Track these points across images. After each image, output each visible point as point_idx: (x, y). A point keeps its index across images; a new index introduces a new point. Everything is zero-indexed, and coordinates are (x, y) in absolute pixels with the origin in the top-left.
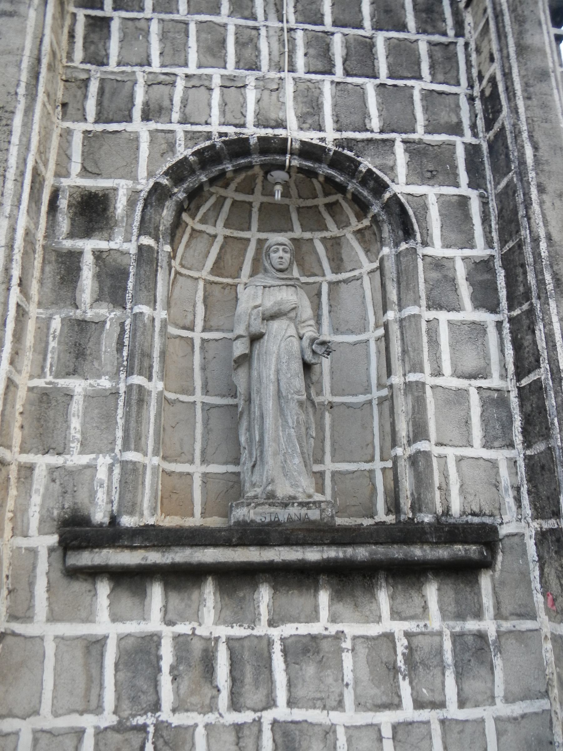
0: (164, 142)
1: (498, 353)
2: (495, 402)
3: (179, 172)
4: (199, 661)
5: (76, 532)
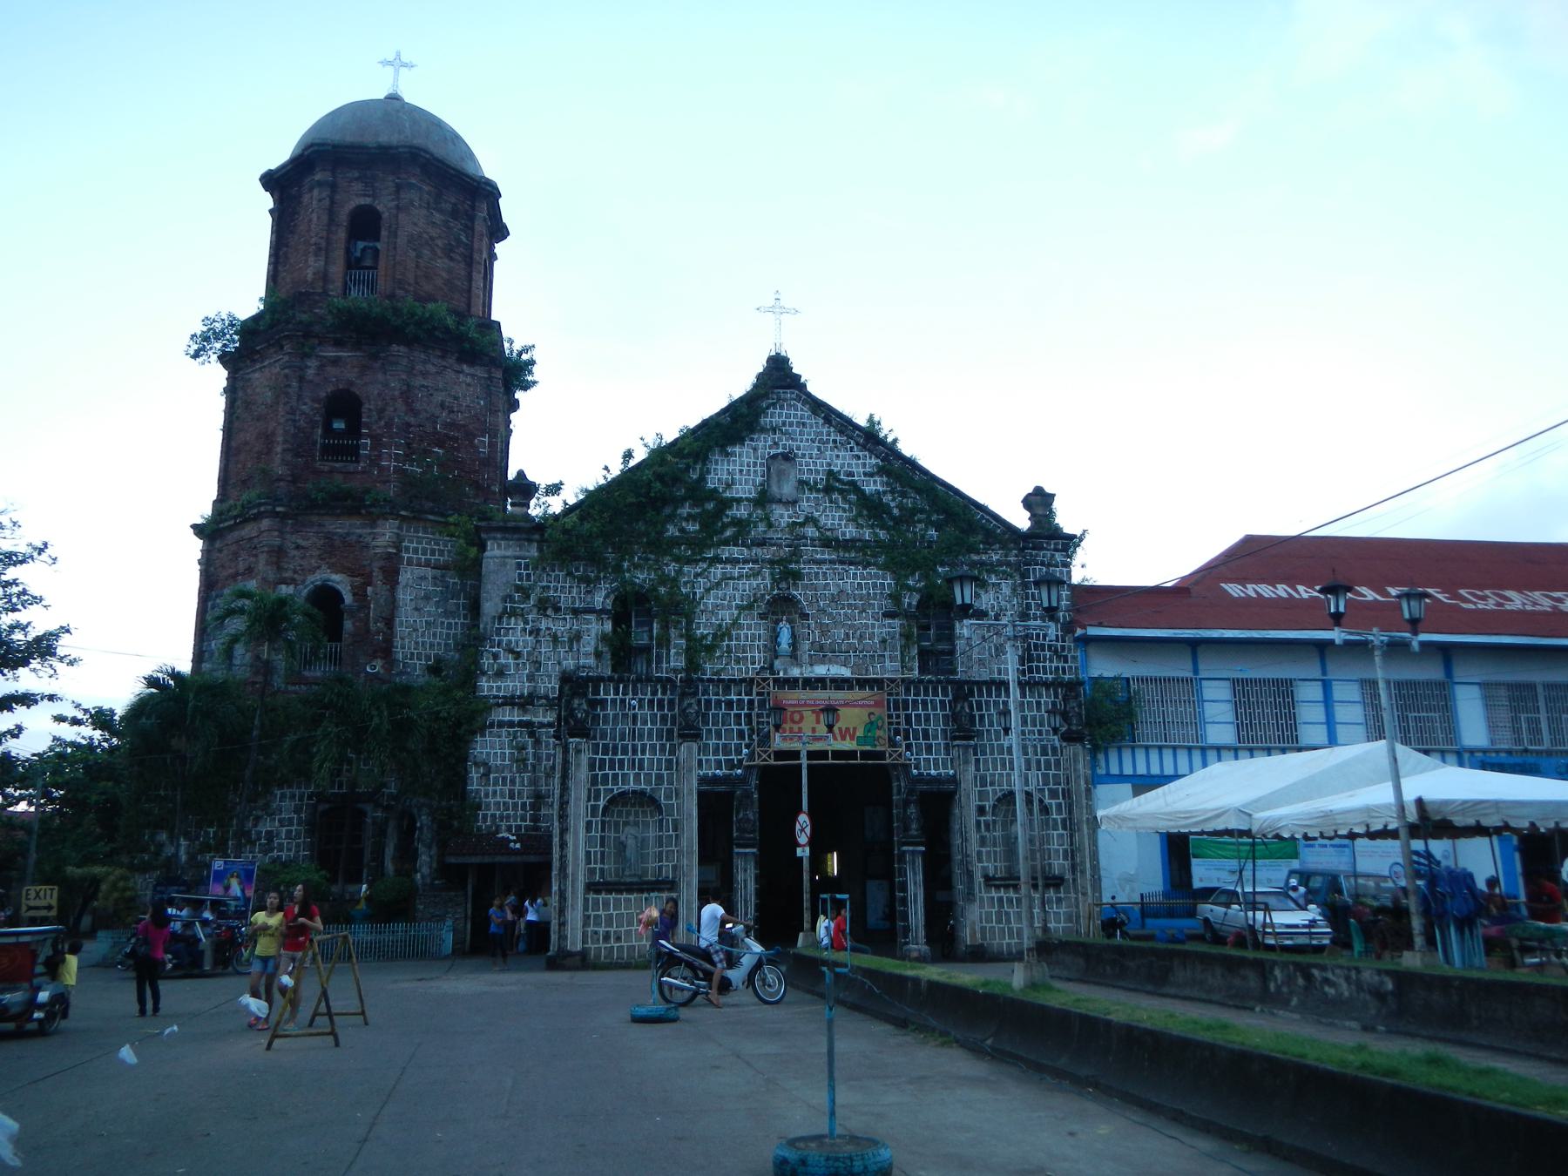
0: (995, 792)
1: (1067, 840)
2: (1065, 851)
3: (999, 800)
4: (1010, 901)
5: (987, 879)
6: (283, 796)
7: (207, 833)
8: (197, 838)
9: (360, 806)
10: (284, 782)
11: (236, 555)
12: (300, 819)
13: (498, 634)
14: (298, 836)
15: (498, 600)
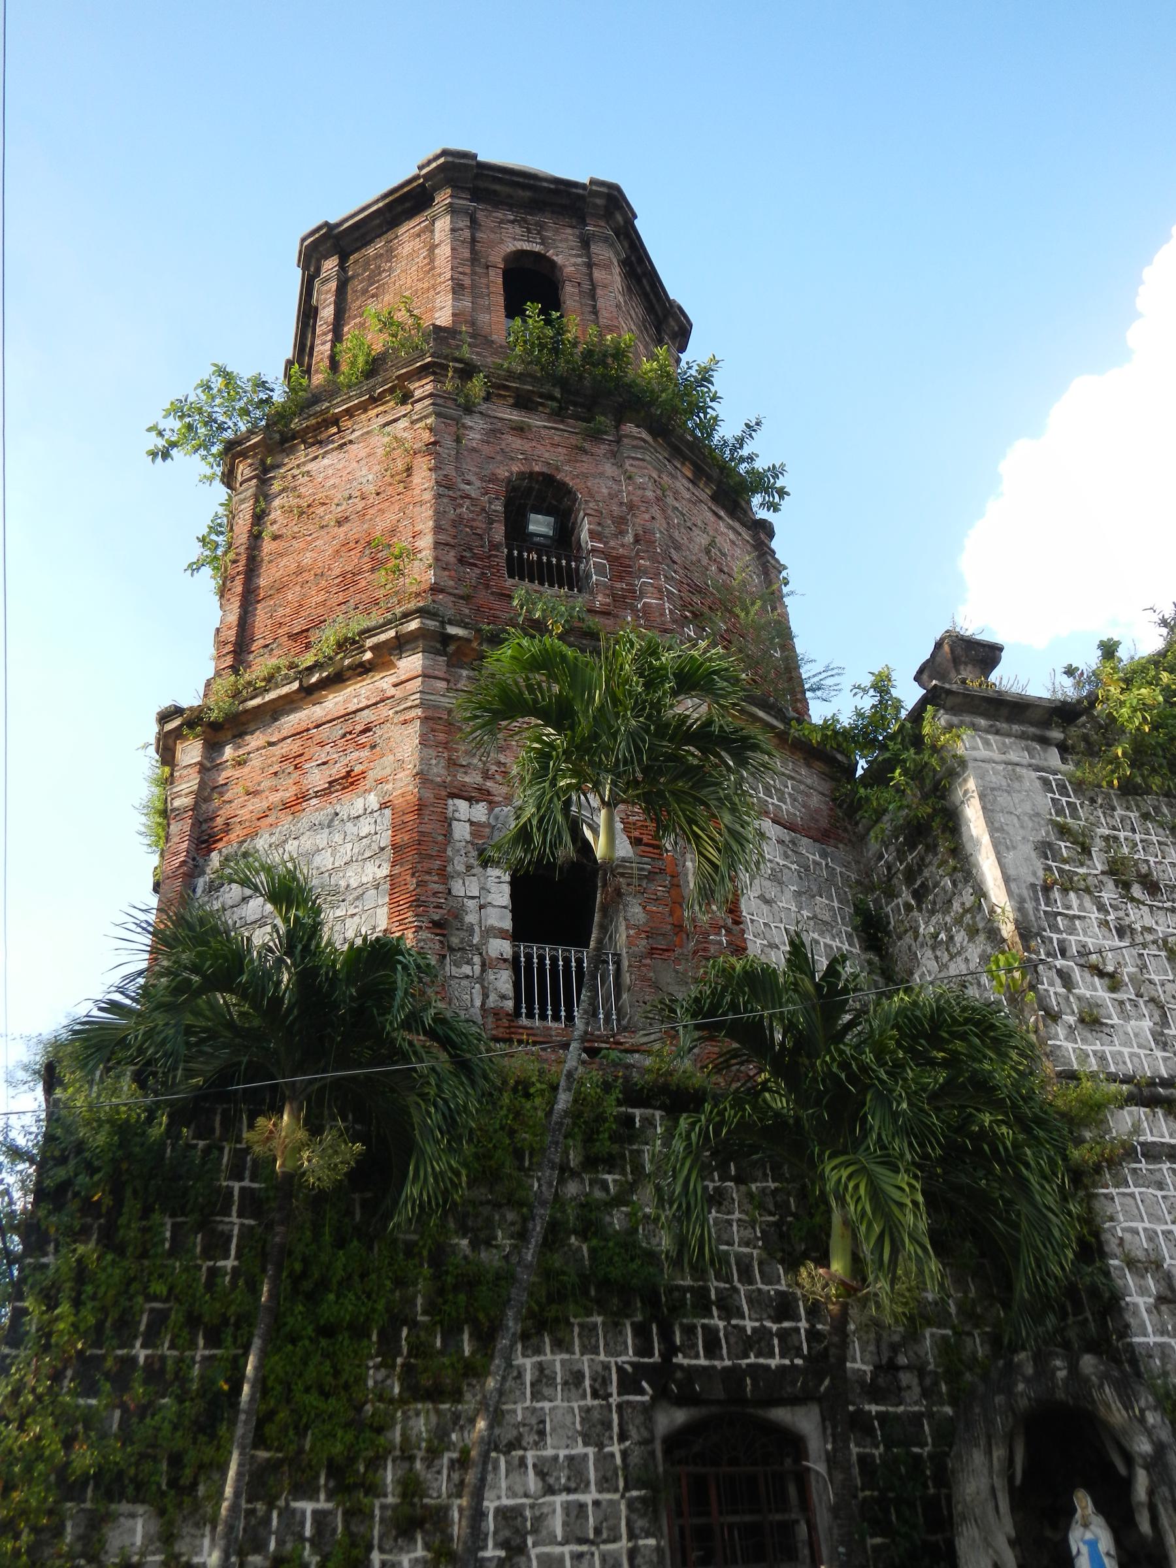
6: (543, 1376)
7: (291, 1519)
8: (259, 1546)
9: (781, 1414)
10: (544, 1326)
11: (296, 762)
12: (604, 1459)
13: (1055, 928)
14: (605, 1533)
15: (1028, 850)
